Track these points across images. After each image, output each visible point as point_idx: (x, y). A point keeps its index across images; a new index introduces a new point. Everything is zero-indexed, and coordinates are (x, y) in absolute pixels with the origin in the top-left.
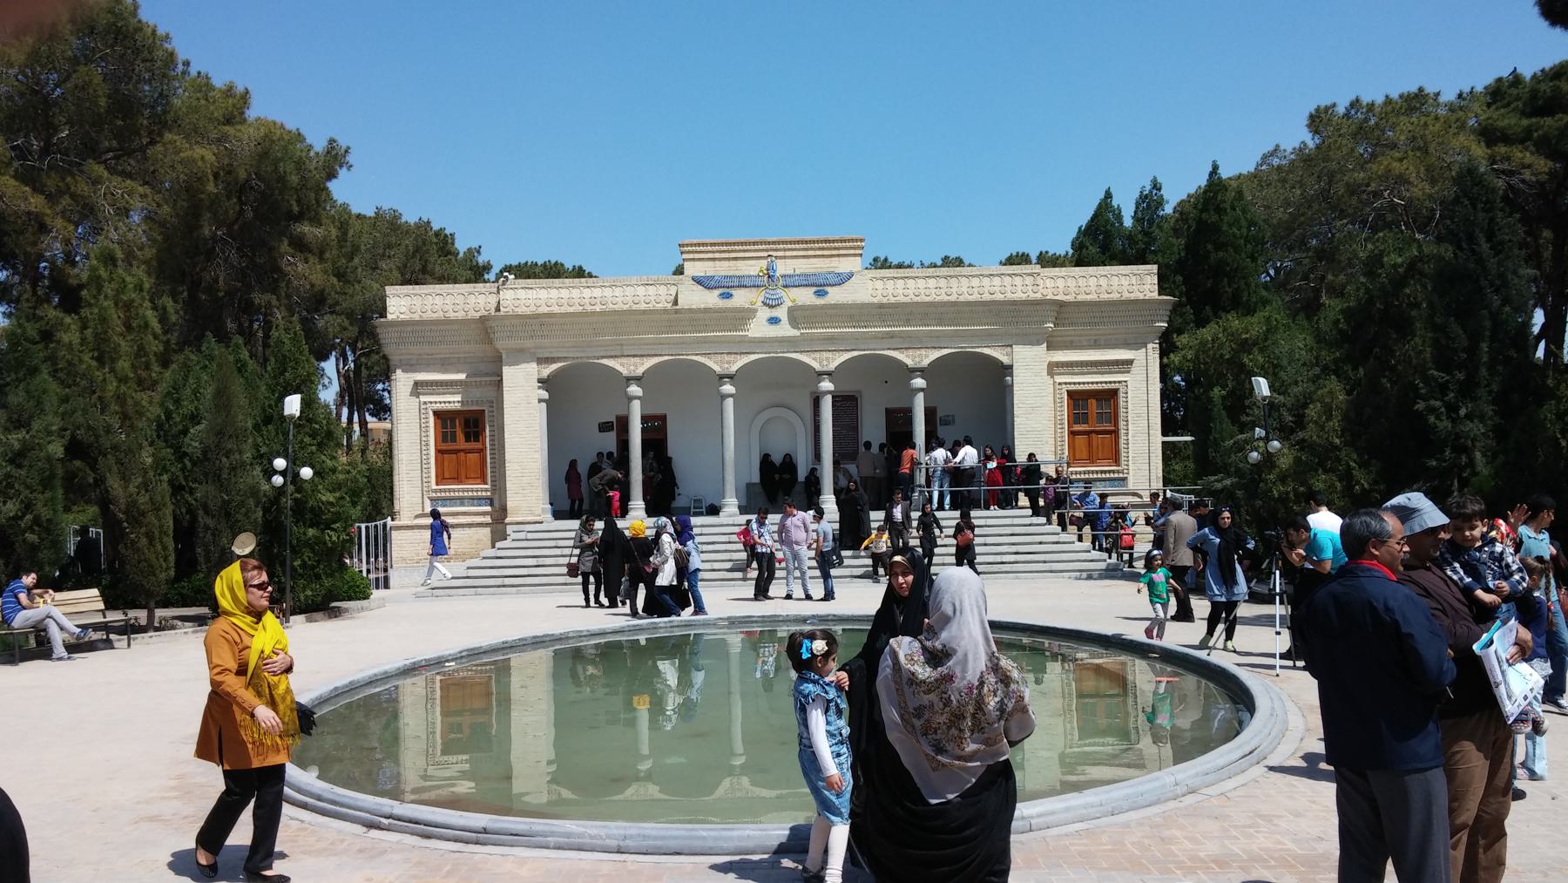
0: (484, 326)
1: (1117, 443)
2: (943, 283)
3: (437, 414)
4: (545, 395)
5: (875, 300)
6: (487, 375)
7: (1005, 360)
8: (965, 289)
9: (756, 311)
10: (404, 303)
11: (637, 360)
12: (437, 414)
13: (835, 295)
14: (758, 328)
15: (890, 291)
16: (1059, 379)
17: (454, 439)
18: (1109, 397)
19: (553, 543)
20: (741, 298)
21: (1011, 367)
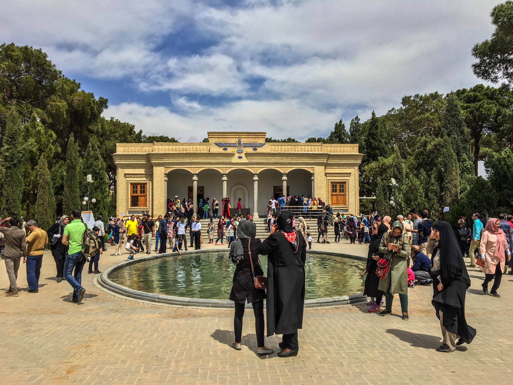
0: (148, 157)
1: (346, 198)
2: (293, 147)
4: (167, 179)
5: (272, 152)
7: (312, 172)
8: (300, 150)
9: (234, 154)
10: (121, 149)
12: (131, 184)
13: (260, 150)
14: (235, 159)
15: (277, 149)
16: (328, 178)
17: (136, 193)
18: (343, 184)
20: (230, 150)
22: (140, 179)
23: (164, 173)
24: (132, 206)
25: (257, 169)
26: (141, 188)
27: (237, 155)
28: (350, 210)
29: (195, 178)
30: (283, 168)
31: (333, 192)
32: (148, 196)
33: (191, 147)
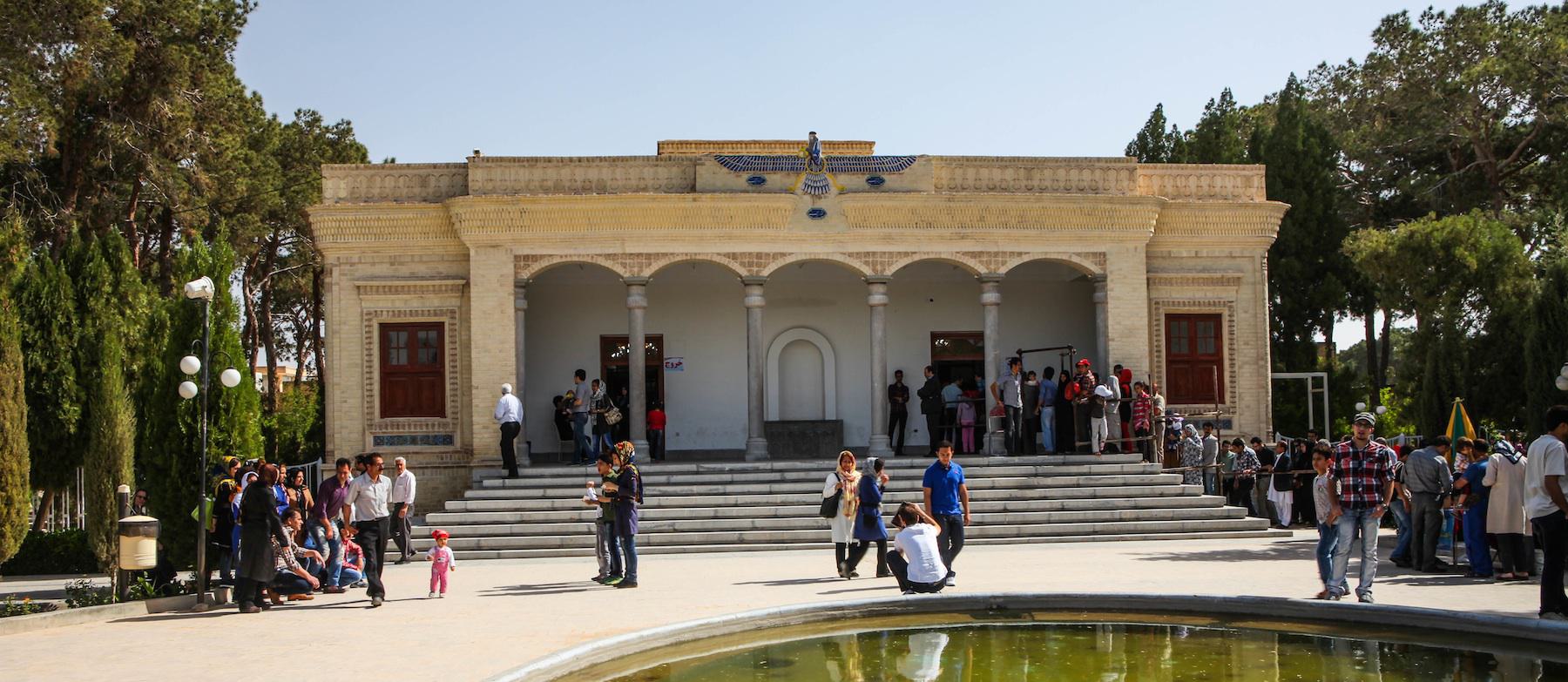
4: (523, 304)
6: (447, 277)
7: (1096, 269)
19: (539, 492)
21: (1104, 278)
23: (511, 280)
24: (384, 414)
27: (807, 203)
28: (1235, 423)
29: (637, 298)
33: (619, 173)
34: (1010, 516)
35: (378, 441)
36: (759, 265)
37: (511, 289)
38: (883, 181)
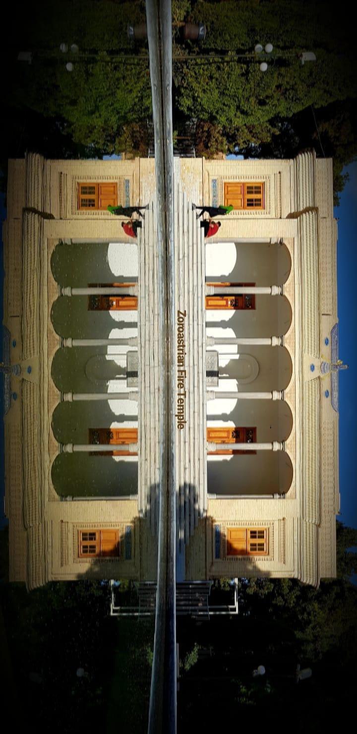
3: (264, 184)
4: (273, 242)
7: (288, 494)
11: (292, 293)
12: (264, 184)
16: (276, 523)
17: (248, 192)
22: (273, 197)
24: (225, 184)
25: (293, 399)
26: (256, 200)
28: (219, 560)
30: (293, 443)
31: (252, 532)
32: (242, 211)
34: (182, 443)
35: (214, 181)
36: (290, 343)
37: (280, 236)
38: (327, 396)
